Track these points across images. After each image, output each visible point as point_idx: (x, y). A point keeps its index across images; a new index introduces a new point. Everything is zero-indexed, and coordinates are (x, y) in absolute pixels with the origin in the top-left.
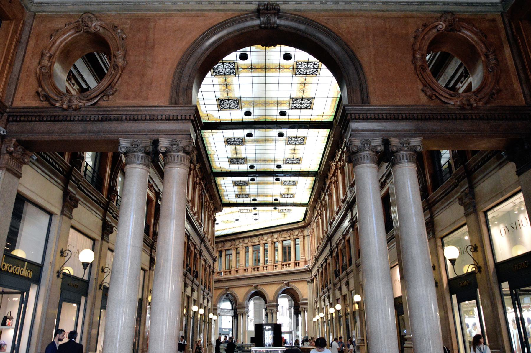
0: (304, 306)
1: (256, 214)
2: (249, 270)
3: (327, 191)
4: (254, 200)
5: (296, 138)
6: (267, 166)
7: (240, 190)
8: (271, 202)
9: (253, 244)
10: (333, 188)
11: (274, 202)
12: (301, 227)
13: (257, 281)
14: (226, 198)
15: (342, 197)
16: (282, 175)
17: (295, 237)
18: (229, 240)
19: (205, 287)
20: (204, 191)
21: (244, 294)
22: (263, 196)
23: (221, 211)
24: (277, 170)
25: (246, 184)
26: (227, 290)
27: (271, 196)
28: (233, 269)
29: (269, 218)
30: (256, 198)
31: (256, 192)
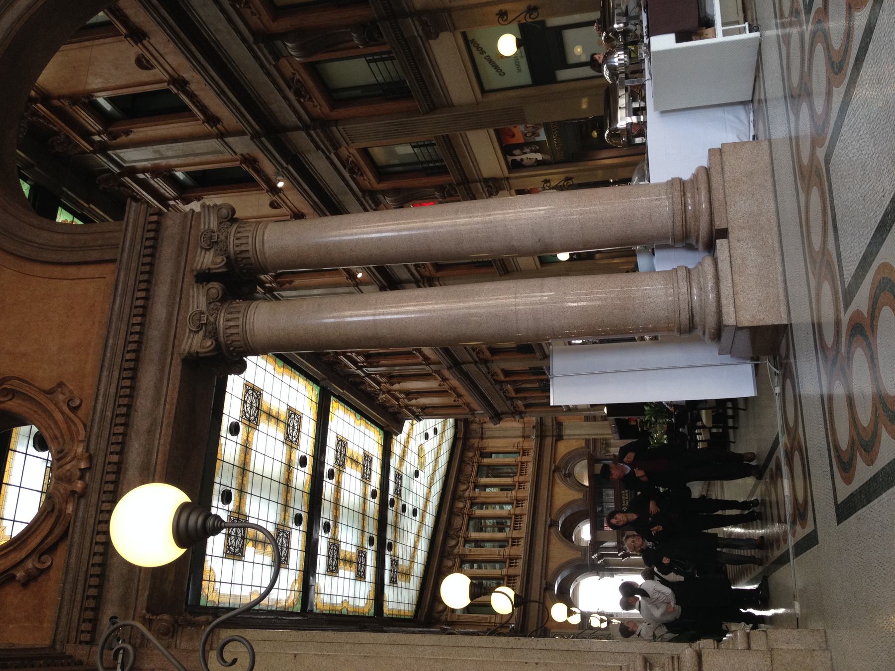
3: (360, 368)
4: (371, 544)
5: (245, 402)
6: (300, 486)
8: (377, 507)
11: (377, 500)
22: (364, 519)
24: (308, 468)
25: (334, 545)
27: (365, 503)
30: (367, 536)
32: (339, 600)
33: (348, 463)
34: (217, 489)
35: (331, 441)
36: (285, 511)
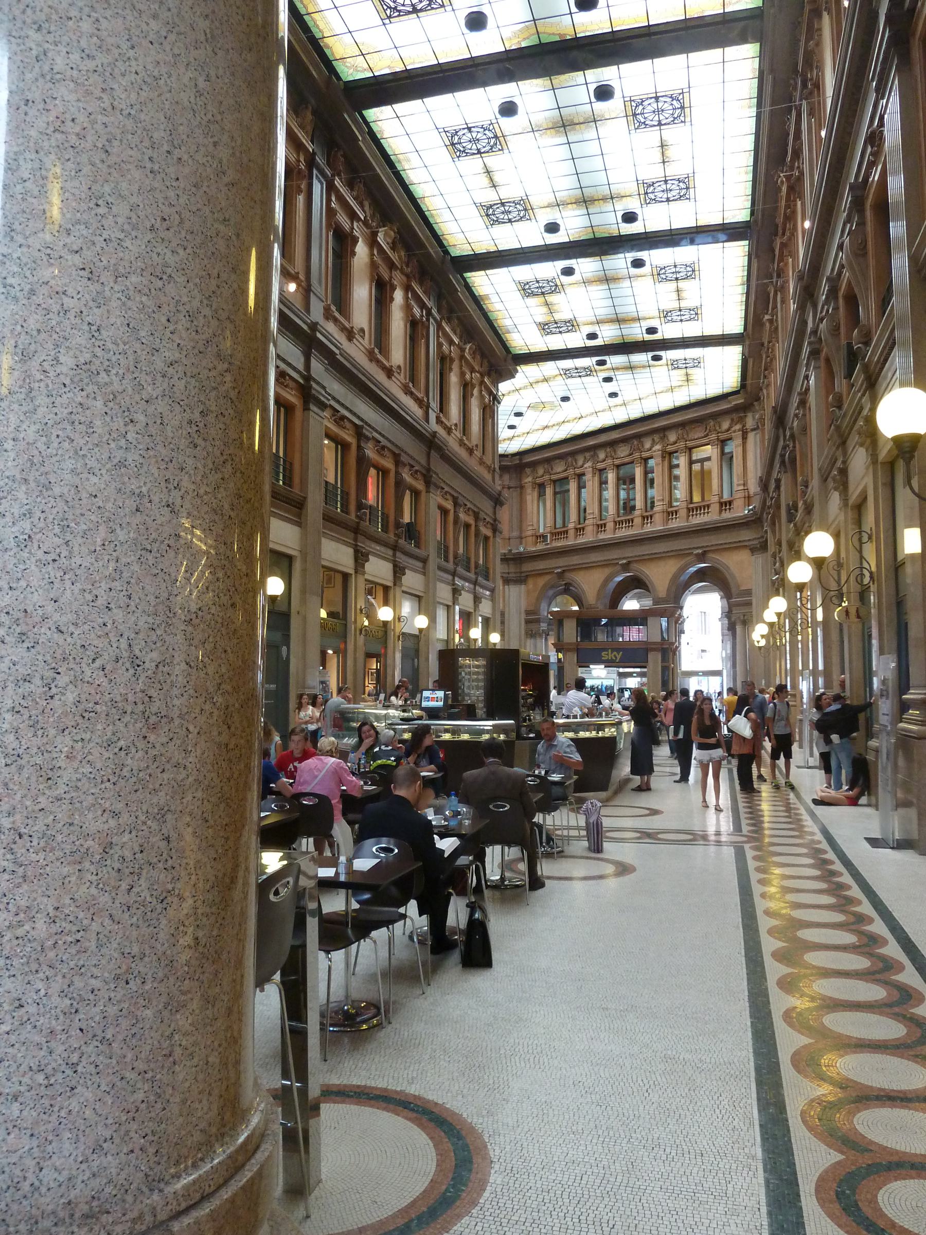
0: (744, 610)
1: (608, 380)
2: (610, 525)
4: (592, 336)
6: (596, 220)
7: (545, 309)
8: (639, 338)
9: (617, 462)
12: (736, 409)
17: (723, 436)
20: (429, 313)
21: (598, 585)
22: (611, 321)
23: (511, 375)
28: (571, 526)
35: (683, 254)
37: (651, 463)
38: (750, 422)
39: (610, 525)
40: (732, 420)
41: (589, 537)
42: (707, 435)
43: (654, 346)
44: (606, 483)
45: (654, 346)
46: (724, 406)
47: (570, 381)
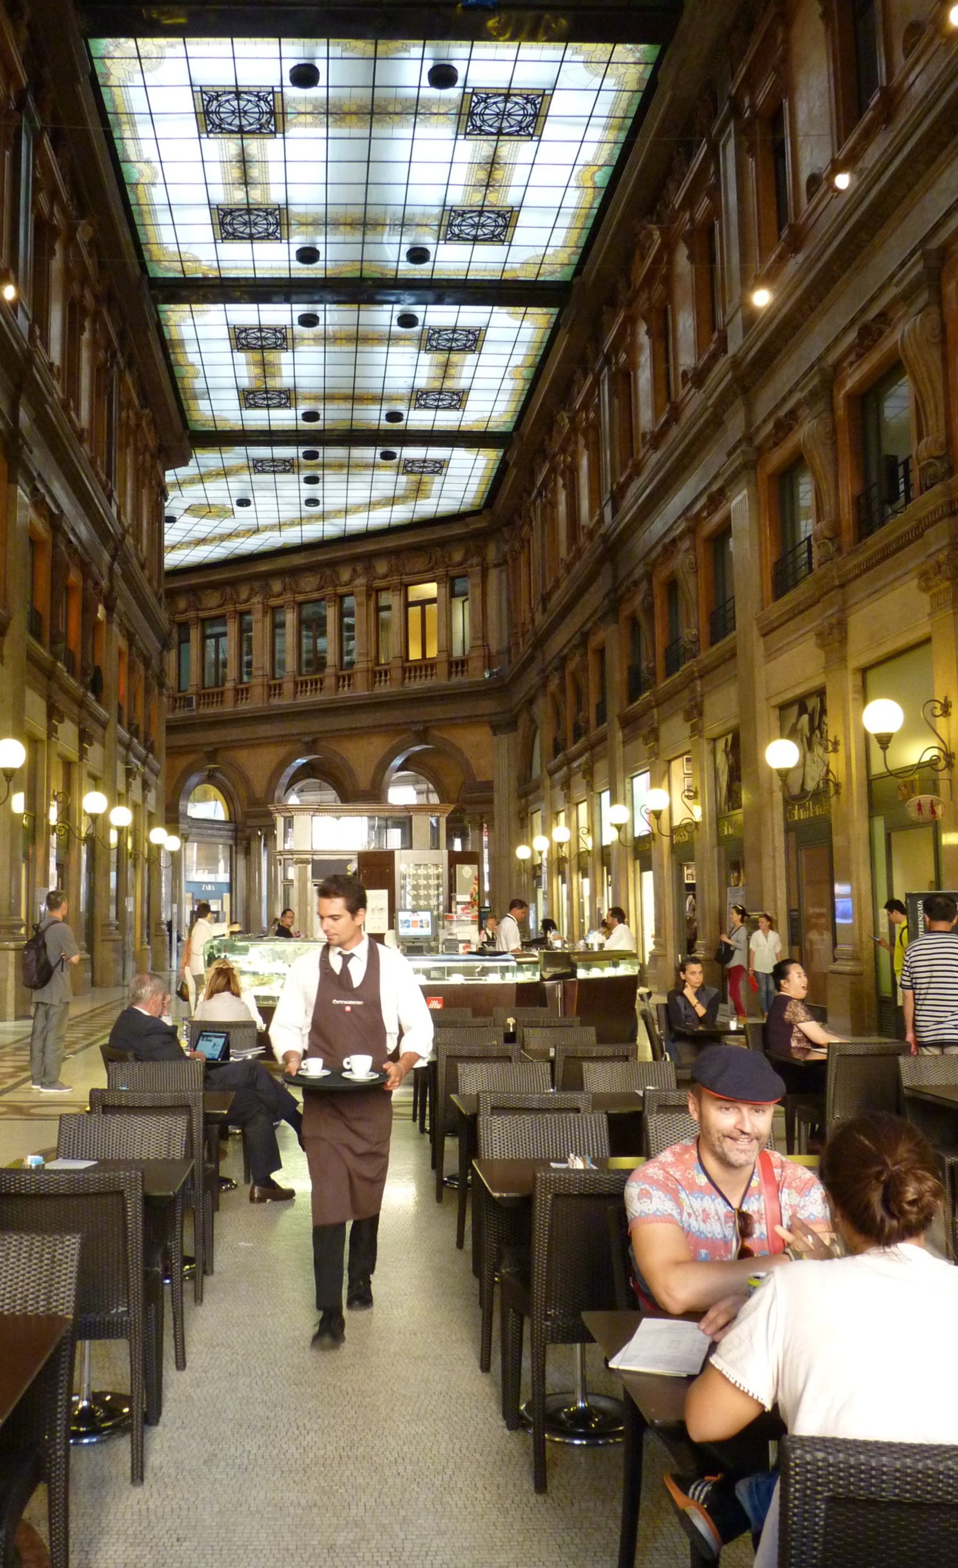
1: (312, 480)
2: (288, 687)
3: (607, 361)
4: (311, 416)
6: (371, 252)
8: (374, 425)
9: (300, 598)
10: (644, 339)
11: (386, 425)
13: (317, 725)
14: (203, 405)
15: (687, 359)
16: (430, 296)
17: (453, 572)
18: (214, 586)
19: (134, 732)
22: (345, 398)
26: (212, 756)
28: (229, 685)
29: (362, 497)
30: (319, 407)
31: (319, 383)
32: (193, 358)
33: (441, 357)
34: (318, 50)
35: (471, 316)
36: (314, 223)
37: (349, 602)
38: (492, 553)
39: (288, 687)
40: (467, 551)
41: (256, 702)
42: (432, 569)
43: (390, 438)
44: (282, 625)
45: (390, 438)
46: (457, 529)
47: (257, 478)
